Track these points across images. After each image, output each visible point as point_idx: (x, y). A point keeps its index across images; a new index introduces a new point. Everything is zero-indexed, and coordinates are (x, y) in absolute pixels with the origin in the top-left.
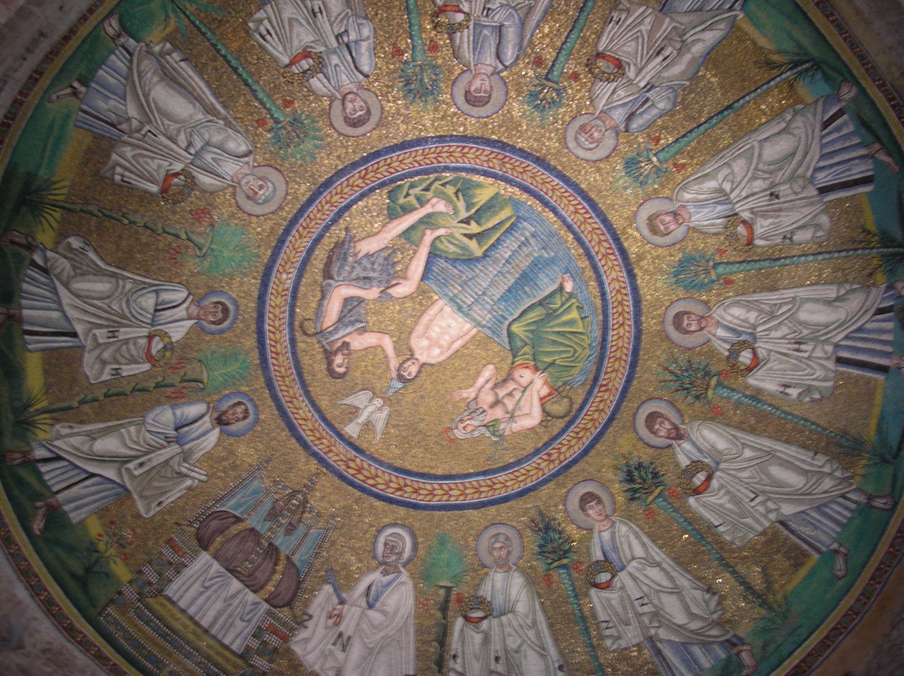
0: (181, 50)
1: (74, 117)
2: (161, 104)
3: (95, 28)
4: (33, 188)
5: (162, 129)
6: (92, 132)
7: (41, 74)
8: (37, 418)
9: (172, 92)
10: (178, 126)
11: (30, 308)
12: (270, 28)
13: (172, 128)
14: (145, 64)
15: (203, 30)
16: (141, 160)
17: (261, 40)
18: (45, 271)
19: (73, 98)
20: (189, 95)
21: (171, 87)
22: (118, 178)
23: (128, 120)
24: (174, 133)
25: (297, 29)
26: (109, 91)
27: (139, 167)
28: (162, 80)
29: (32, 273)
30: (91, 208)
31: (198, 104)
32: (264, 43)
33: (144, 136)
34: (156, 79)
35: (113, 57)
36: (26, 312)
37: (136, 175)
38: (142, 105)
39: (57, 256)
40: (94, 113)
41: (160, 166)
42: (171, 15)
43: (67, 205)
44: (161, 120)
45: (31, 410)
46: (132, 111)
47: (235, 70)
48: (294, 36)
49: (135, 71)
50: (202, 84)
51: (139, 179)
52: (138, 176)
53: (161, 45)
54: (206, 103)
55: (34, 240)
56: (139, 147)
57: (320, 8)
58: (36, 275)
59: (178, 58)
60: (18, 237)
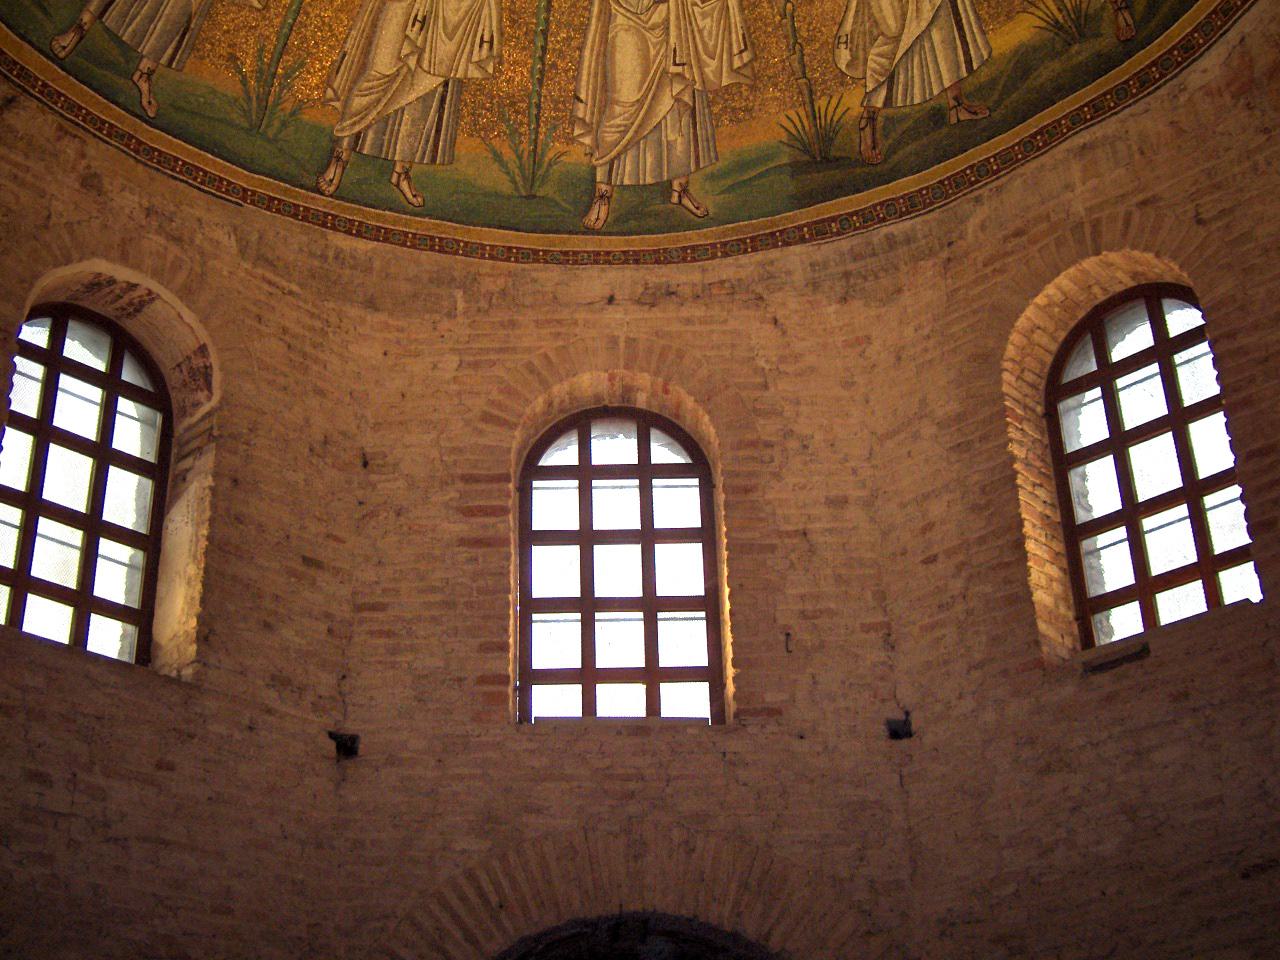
0: (572, 111)
1: (708, 170)
2: (638, 77)
3: (610, 234)
4: (806, 158)
5: (663, 51)
6: (713, 136)
7: (684, 249)
8: (1069, 6)
9: (618, 76)
10: (648, 34)
11: (940, 77)
12: (477, 48)
13: (654, 40)
14: (610, 138)
15: (535, 112)
16: (711, 43)
17: (495, 42)
18: (891, 79)
19: (691, 189)
20: (609, 55)
21: (614, 82)
22: (746, 56)
23: (677, 99)
24: (658, 31)
25: (454, 19)
26: (661, 153)
27: (720, 41)
28: (617, 102)
29: (900, 97)
30: (796, 65)
31: (610, 36)
32: (495, 35)
33: (684, 64)
34: (618, 109)
35: (626, 182)
36: (947, 84)
37: (730, 39)
38: (653, 99)
39: (869, 73)
40: (692, 149)
41: (704, 16)
42: (546, 159)
43: (807, 100)
44: (654, 62)
45: (1059, 17)
46: (666, 103)
47: (545, 33)
48: (461, 13)
49: (624, 142)
50: (587, 53)
51: (733, 26)
52: (730, 33)
53: (581, 140)
54: (602, 27)
55: (862, 118)
56: (699, 60)
57: (413, 25)
58: (900, 87)
59: (581, 106)
60: (866, 143)
